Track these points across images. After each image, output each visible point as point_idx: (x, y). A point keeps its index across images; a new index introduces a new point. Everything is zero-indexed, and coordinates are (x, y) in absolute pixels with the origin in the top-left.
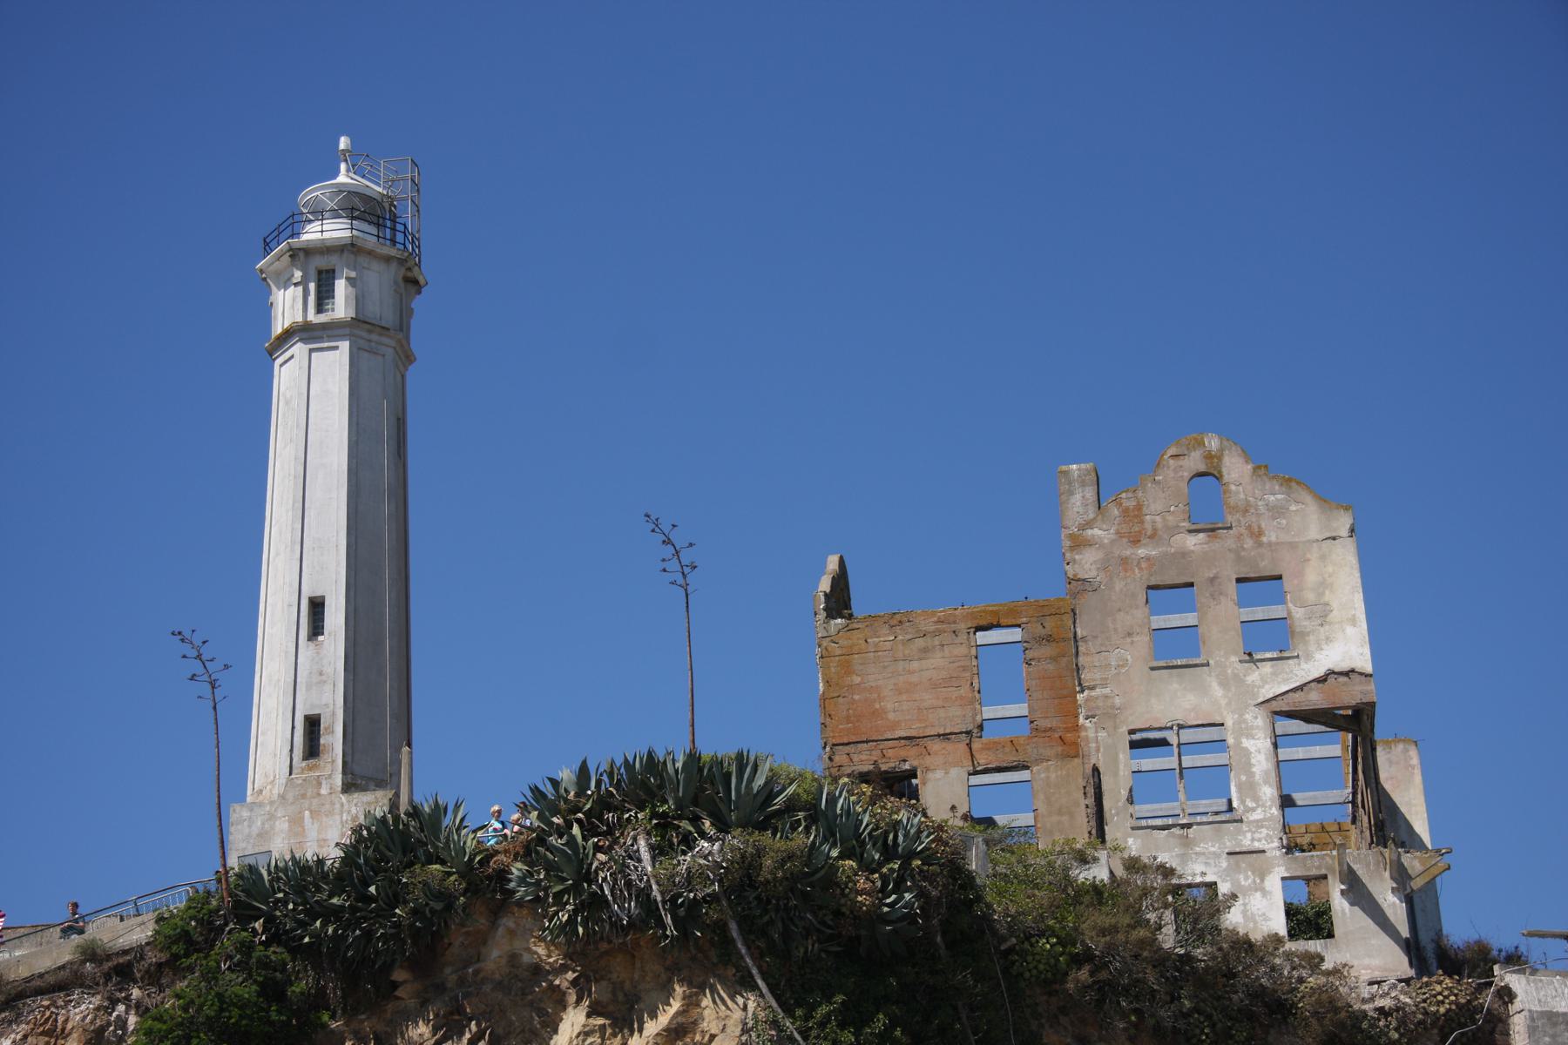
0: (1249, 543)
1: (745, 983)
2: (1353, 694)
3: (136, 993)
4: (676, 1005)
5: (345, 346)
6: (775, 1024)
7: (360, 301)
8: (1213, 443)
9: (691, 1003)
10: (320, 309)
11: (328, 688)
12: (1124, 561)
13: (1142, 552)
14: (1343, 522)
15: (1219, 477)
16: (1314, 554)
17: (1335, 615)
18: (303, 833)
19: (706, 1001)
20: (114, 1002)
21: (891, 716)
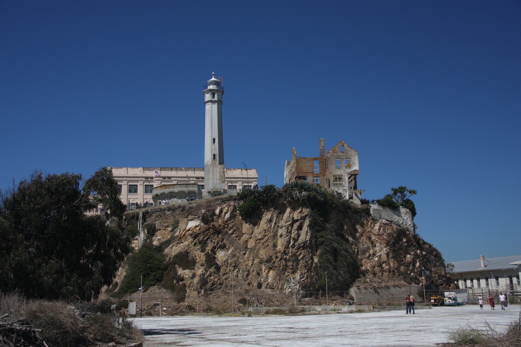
0: (347, 154)
1: (307, 207)
2: (356, 173)
3: (237, 201)
4: (300, 209)
5: (217, 104)
6: (311, 212)
7: (218, 98)
8: (343, 142)
9: (302, 209)
10: (213, 98)
11: (216, 151)
12: (333, 155)
13: (335, 154)
14: (357, 153)
15: (344, 146)
16: (353, 156)
17: (355, 164)
18: (214, 169)
19: (304, 209)
20: (235, 202)
21: (304, 170)
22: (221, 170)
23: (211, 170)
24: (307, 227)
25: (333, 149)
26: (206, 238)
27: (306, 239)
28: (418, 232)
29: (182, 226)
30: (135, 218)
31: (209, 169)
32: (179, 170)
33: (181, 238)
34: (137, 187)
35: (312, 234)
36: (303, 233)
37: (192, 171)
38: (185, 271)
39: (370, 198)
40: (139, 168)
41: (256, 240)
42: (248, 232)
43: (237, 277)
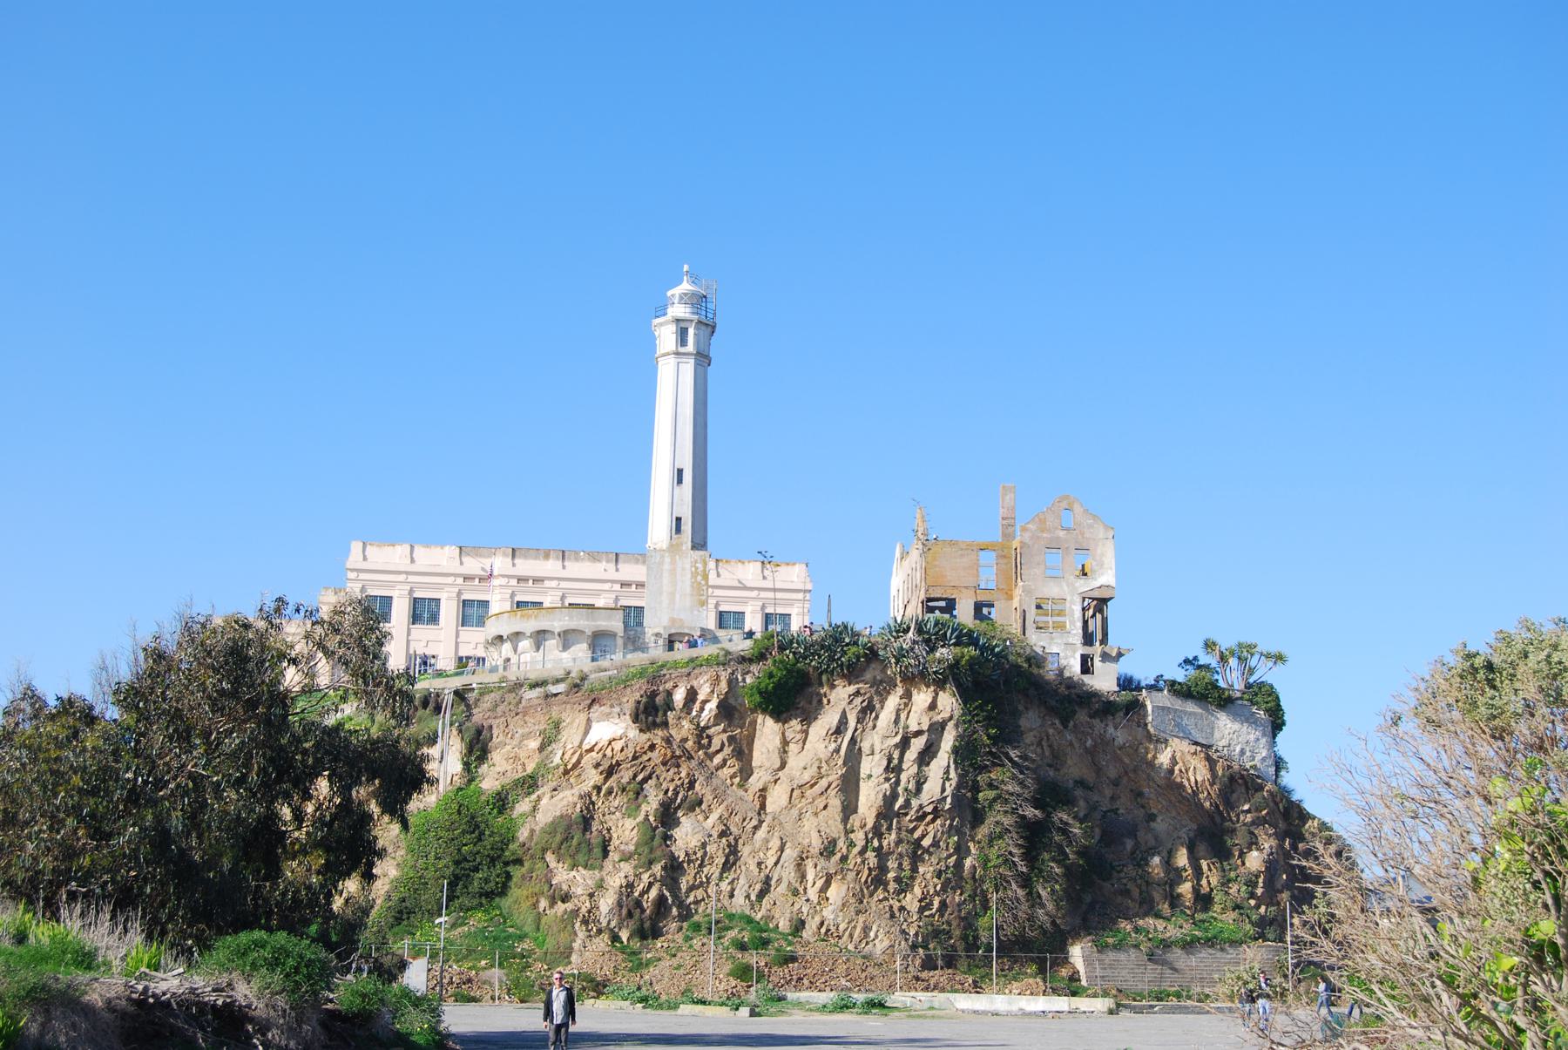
7: (697, 343)
12: (1038, 537)
13: (1045, 535)
17: (1105, 566)
22: (697, 568)
23: (666, 567)
24: (947, 755)
25: (1040, 520)
26: (640, 777)
27: (943, 790)
28: (1287, 779)
29: (570, 737)
30: (431, 705)
31: (661, 563)
32: (570, 559)
33: (566, 772)
34: (438, 606)
35: (961, 777)
37: (608, 561)
38: (574, 873)
39: (1145, 676)
40: (447, 548)
41: (793, 790)
42: (767, 764)
43: (732, 896)
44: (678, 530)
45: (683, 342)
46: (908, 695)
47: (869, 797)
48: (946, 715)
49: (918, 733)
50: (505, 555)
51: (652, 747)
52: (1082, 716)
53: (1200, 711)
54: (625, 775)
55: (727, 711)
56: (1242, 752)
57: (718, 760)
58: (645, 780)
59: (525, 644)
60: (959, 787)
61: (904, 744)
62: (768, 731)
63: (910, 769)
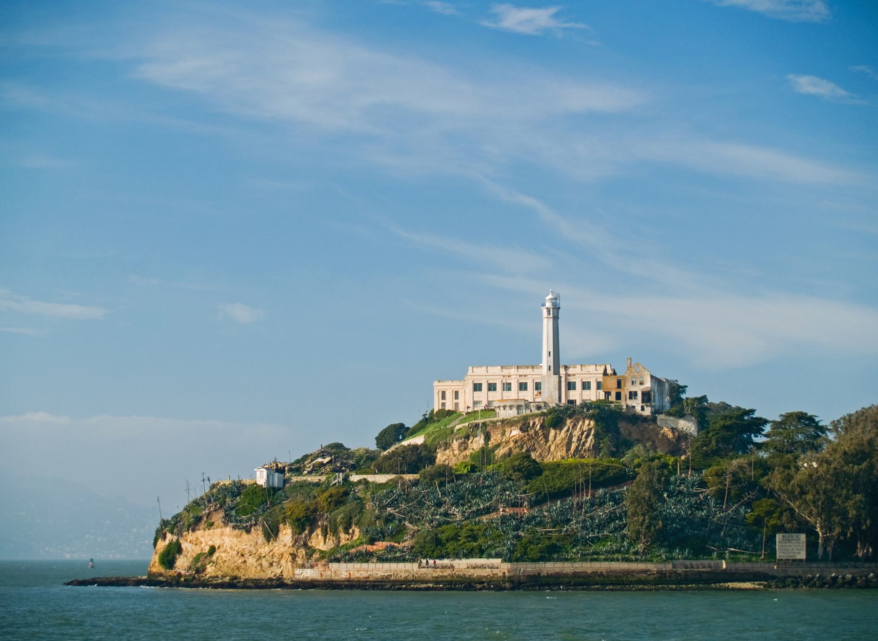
7: (553, 314)
26: (523, 444)
29: (507, 434)
33: (506, 443)
35: (595, 441)
36: (589, 440)
44: (550, 370)
45: (549, 314)
46: (584, 422)
47: (573, 446)
48: (592, 426)
49: (585, 431)
50: (515, 368)
51: (525, 436)
52: (639, 422)
53: (674, 419)
54: (519, 443)
55: (542, 427)
56: (687, 429)
57: (540, 439)
58: (524, 444)
59: (502, 408)
60: (594, 443)
61: (582, 434)
62: (552, 432)
63: (583, 440)
